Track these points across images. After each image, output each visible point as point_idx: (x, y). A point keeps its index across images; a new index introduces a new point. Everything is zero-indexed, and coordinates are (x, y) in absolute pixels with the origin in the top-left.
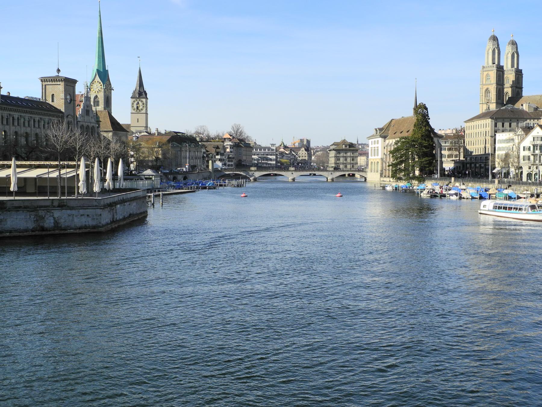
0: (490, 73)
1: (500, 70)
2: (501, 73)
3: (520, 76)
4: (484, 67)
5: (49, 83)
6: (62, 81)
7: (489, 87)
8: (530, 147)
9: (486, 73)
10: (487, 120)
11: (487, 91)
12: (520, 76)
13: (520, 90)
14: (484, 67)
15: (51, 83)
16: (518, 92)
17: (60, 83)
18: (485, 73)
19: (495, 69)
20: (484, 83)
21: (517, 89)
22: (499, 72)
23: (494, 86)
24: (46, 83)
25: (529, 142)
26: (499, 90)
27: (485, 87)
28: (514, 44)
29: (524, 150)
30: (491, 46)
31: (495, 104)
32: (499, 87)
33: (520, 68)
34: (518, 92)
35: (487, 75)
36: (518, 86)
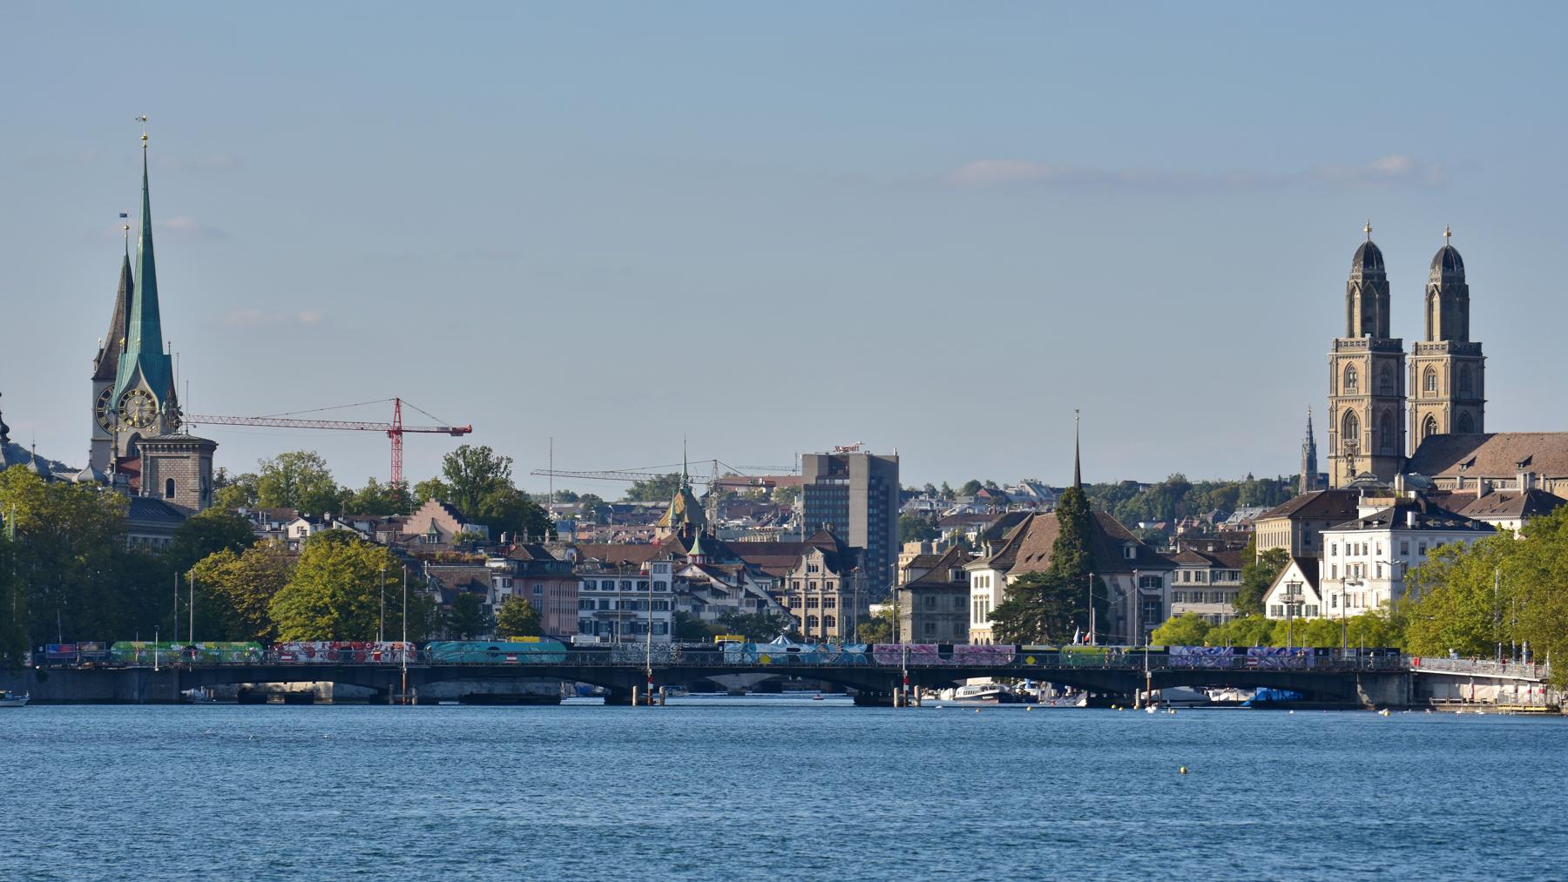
0: (1355, 362)
1: (1387, 354)
2: (1393, 362)
3: (1472, 366)
5: (160, 453)
6: (194, 450)
7: (1354, 406)
9: (1346, 361)
11: (1350, 419)
12: (1472, 366)
13: (1472, 410)
15: (166, 454)
17: (190, 454)
18: (1343, 363)
20: (1340, 393)
21: (1460, 408)
22: (1381, 363)
23: (1367, 402)
24: (155, 454)
28: (1450, 261)
31: (1369, 461)
32: (1384, 406)
35: (1349, 368)
36: (1465, 396)
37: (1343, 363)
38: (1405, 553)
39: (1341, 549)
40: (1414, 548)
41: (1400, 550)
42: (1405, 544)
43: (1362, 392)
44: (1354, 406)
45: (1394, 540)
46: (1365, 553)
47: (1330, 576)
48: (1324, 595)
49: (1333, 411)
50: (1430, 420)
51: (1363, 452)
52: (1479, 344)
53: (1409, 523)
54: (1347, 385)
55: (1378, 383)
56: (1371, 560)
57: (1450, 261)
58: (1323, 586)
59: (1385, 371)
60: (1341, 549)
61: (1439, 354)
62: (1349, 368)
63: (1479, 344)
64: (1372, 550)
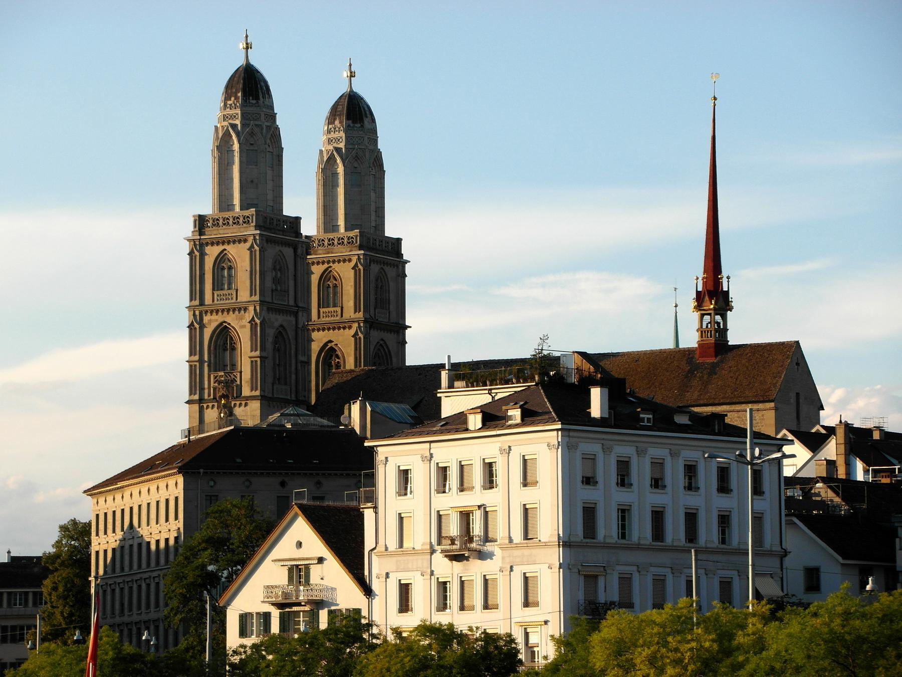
2: (288, 252)
4: (201, 222)
7: (231, 319)
8: (267, 616)
10: (171, 482)
11: (224, 339)
12: (391, 272)
13: (390, 338)
14: (201, 222)
16: (382, 346)
18: (213, 252)
19: (251, 231)
21: (376, 335)
22: (272, 250)
25: (260, 595)
26: (280, 335)
27: (212, 322)
28: (353, 113)
29: (243, 633)
30: (238, 122)
31: (255, 406)
32: (278, 320)
33: (391, 231)
34: (382, 346)
36: (382, 318)
37: (213, 252)
38: (588, 481)
39: (421, 478)
40: (606, 471)
41: (579, 478)
42: (590, 459)
43: (244, 295)
44: (231, 319)
45: (568, 447)
46: (490, 481)
47: (393, 545)
48: (376, 586)
49: (195, 328)
50: (330, 353)
51: (246, 391)
52: (398, 241)
53: (596, 411)
54: (217, 285)
55: (269, 283)
56: (504, 503)
57: (353, 113)
58: (376, 567)
59: (279, 266)
60: (421, 478)
61: (341, 251)
62: (223, 263)
63: (398, 241)
64: (509, 472)
